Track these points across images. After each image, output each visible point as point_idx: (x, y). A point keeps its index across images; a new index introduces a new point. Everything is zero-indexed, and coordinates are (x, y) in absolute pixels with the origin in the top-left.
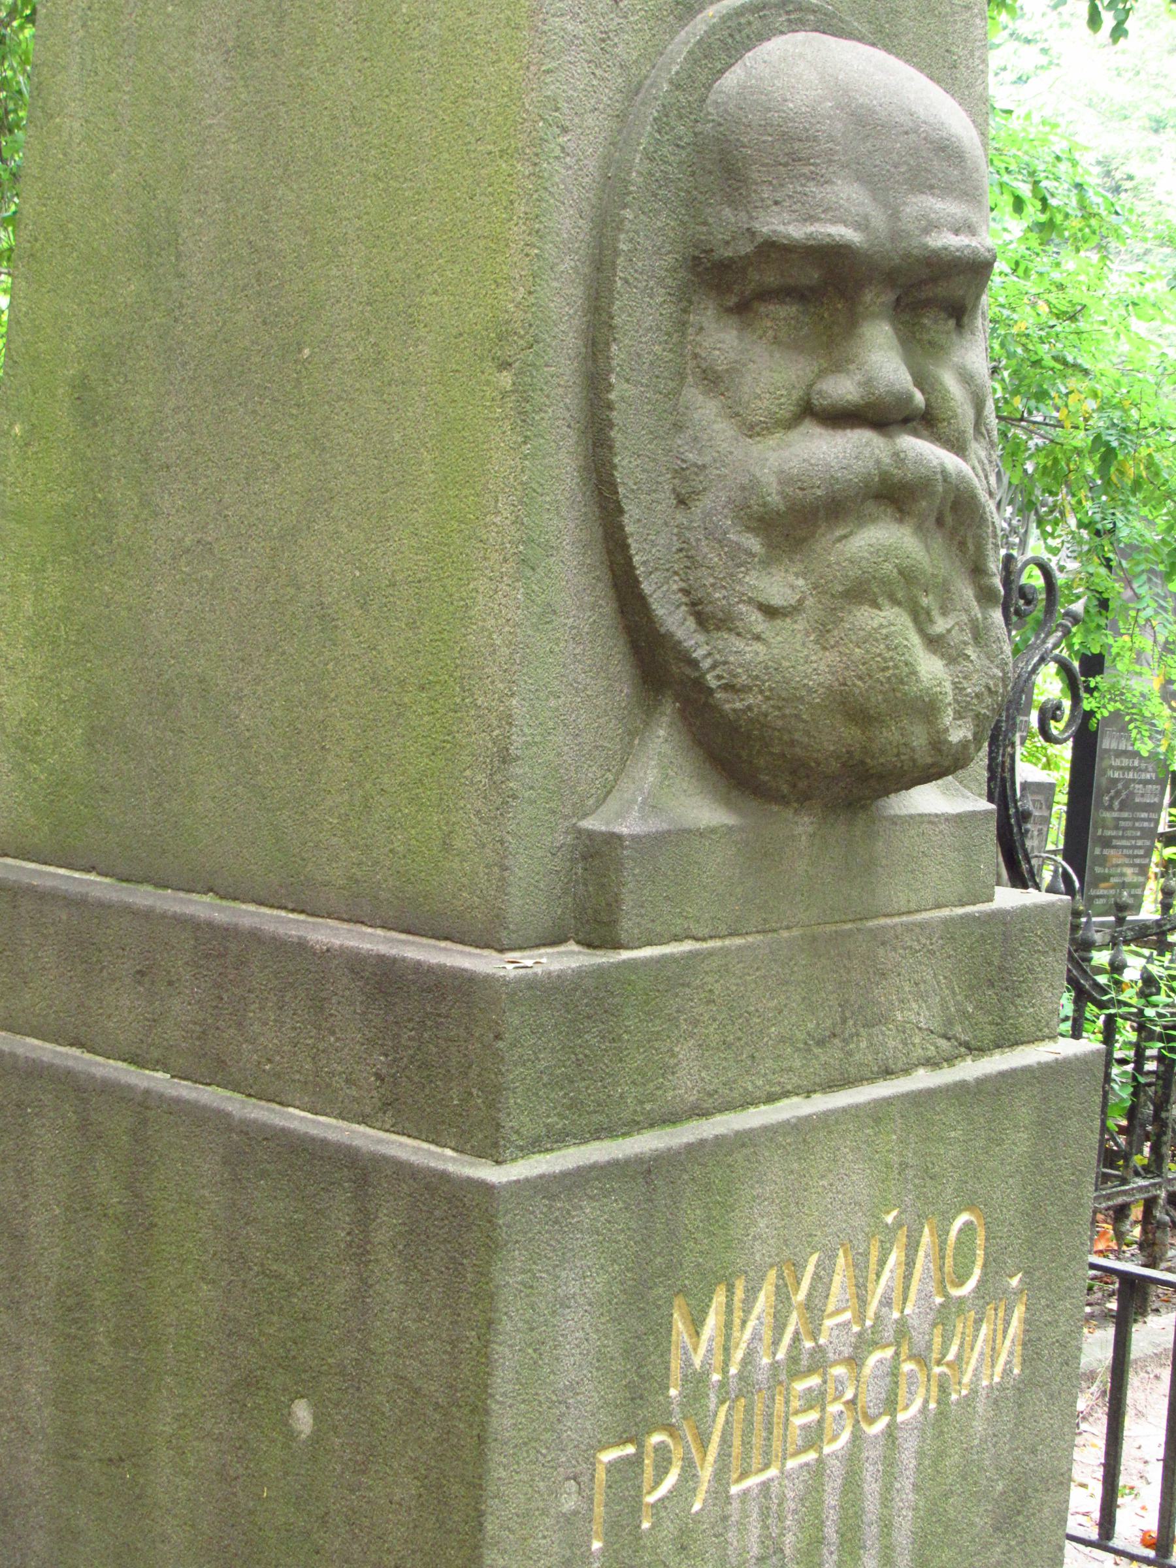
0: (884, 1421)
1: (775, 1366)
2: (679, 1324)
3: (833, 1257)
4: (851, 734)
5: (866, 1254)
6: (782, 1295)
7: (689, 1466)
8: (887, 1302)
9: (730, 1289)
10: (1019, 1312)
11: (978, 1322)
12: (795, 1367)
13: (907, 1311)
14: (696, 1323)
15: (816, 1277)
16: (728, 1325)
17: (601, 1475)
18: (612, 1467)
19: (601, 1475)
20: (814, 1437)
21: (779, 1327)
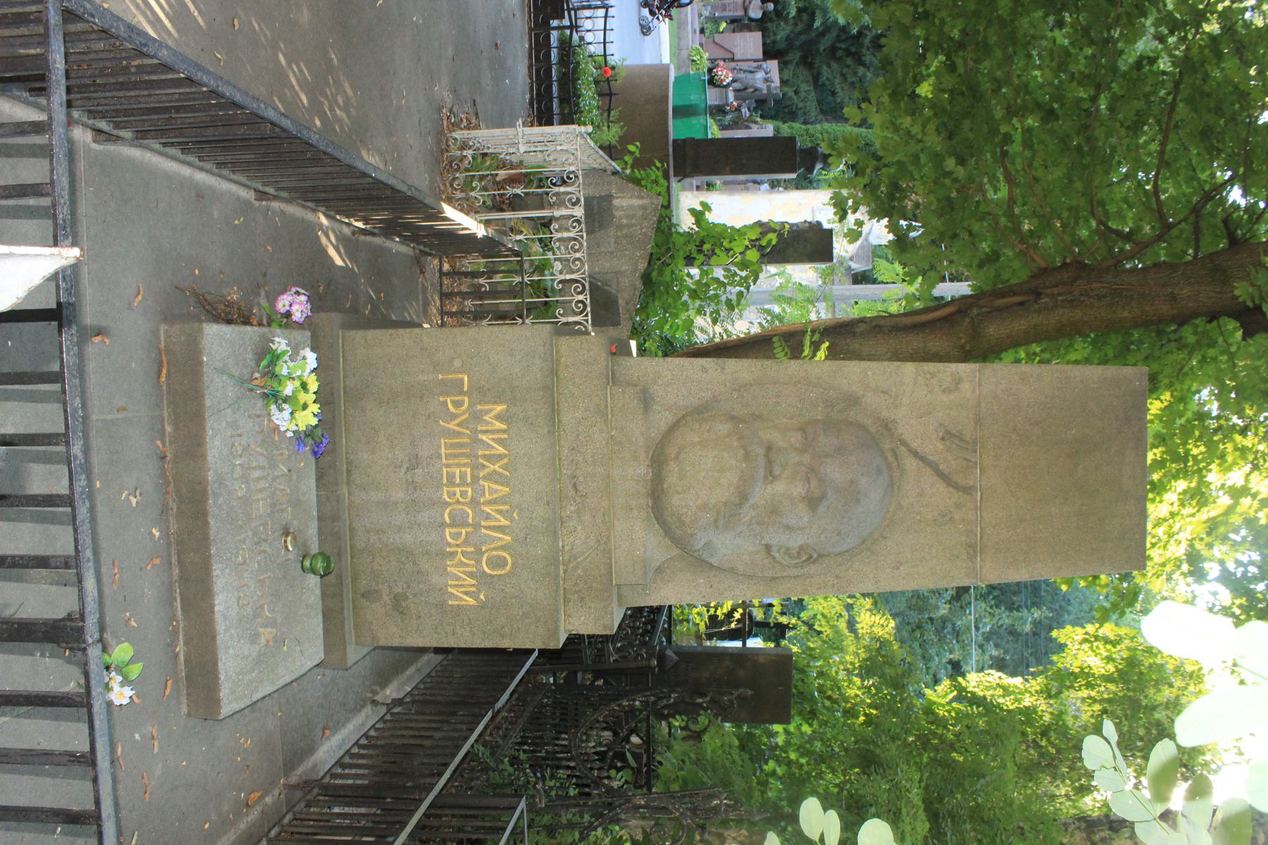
0: (448, 520)
1: (477, 457)
2: (500, 408)
3: (506, 484)
4: (673, 455)
5: (505, 503)
6: (500, 457)
7: (454, 416)
8: (488, 517)
9: (504, 431)
10: (471, 601)
11: (471, 575)
12: (476, 467)
13: (483, 531)
14: (499, 417)
15: (501, 475)
16: (492, 432)
17: (460, 376)
18: (462, 380)
19: (460, 376)
20: (451, 477)
21: (488, 458)
